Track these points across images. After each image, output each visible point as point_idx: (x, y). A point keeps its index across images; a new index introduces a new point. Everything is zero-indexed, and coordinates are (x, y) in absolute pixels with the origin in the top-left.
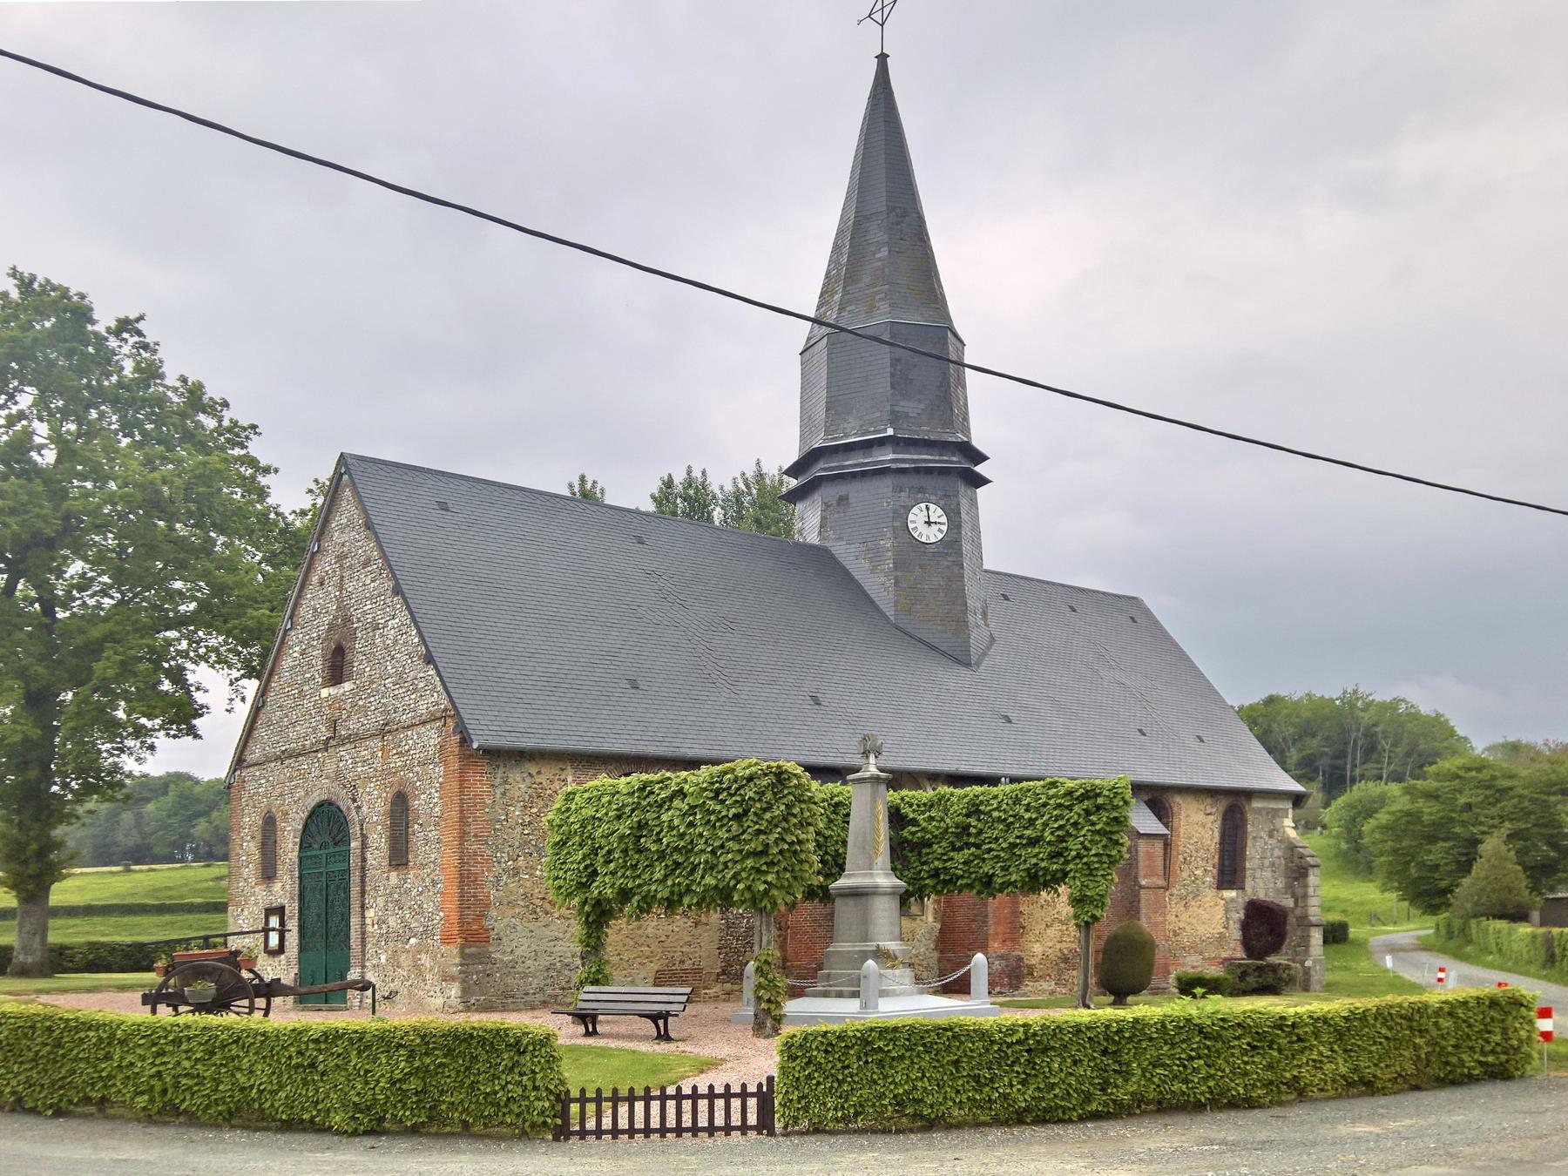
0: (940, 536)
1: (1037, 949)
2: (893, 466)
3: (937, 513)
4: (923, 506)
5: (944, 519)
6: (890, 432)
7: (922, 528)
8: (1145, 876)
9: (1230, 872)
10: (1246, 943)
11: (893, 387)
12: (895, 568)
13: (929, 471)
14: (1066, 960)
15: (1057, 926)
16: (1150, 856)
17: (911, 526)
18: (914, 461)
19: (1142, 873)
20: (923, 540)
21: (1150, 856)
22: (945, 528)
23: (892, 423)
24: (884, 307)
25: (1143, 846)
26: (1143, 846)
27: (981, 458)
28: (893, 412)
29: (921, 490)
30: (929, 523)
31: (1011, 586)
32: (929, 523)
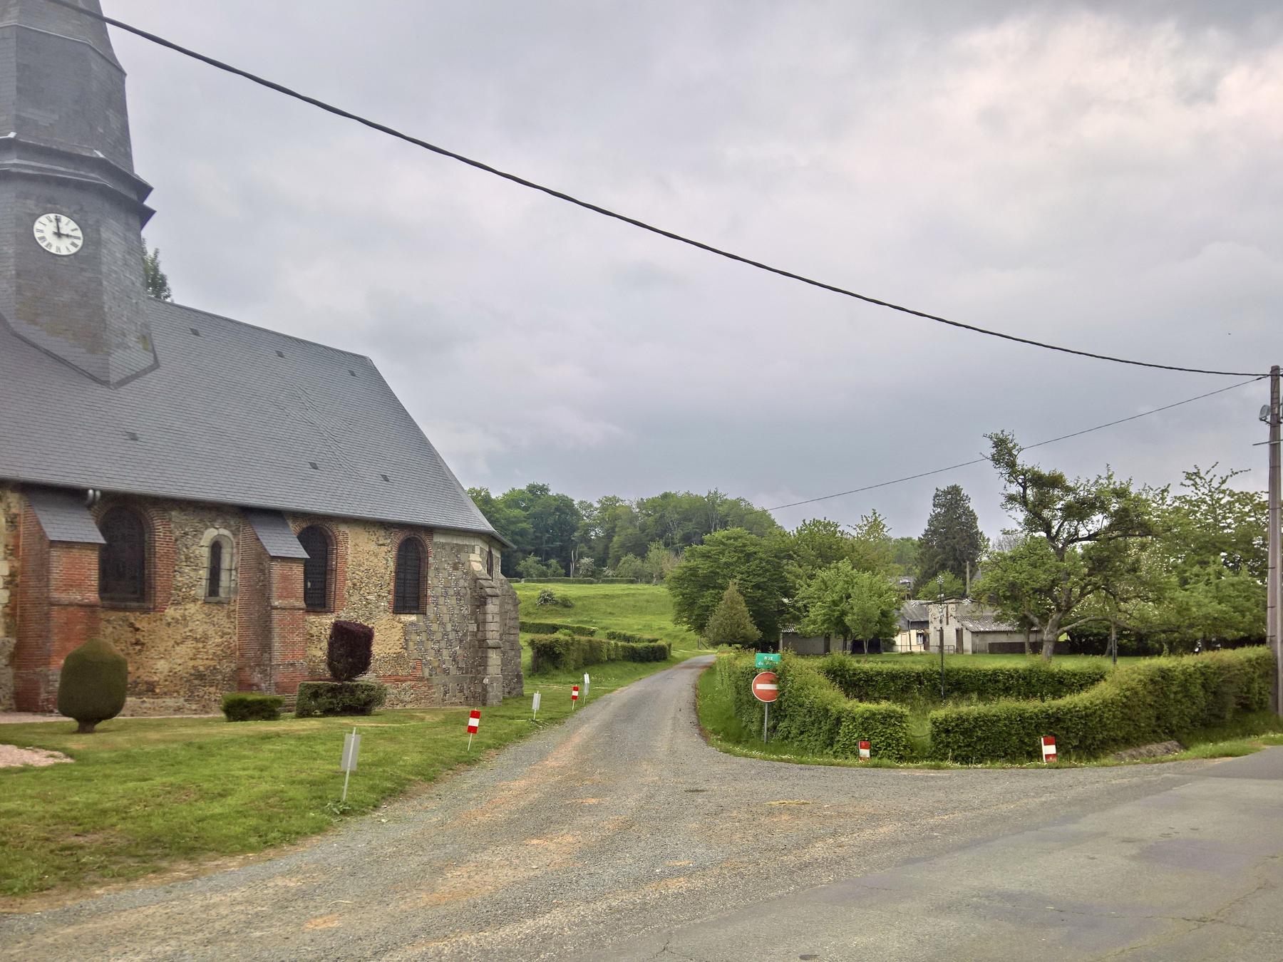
0: (74, 250)
1: (162, 665)
2: (14, 170)
3: (68, 225)
4: (52, 216)
5: (79, 233)
6: (12, 135)
7: (51, 238)
8: (280, 597)
9: (318, 598)
10: (331, 662)
11: (19, 90)
12: (18, 275)
13: (63, 183)
14: (200, 676)
15: (190, 643)
16: (285, 578)
17: (37, 235)
18: (40, 169)
19: (275, 594)
20: (53, 250)
21: (285, 578)
22: (80, 243)
23: (17, 129)
24: (14, 12)
25: (277, 569)
26: (277, 569)
27: (145, 190)
28: (18, 117)
29: (51, 200)
30: (59, 234)
31: (201, 324)
32: (59, 234)
